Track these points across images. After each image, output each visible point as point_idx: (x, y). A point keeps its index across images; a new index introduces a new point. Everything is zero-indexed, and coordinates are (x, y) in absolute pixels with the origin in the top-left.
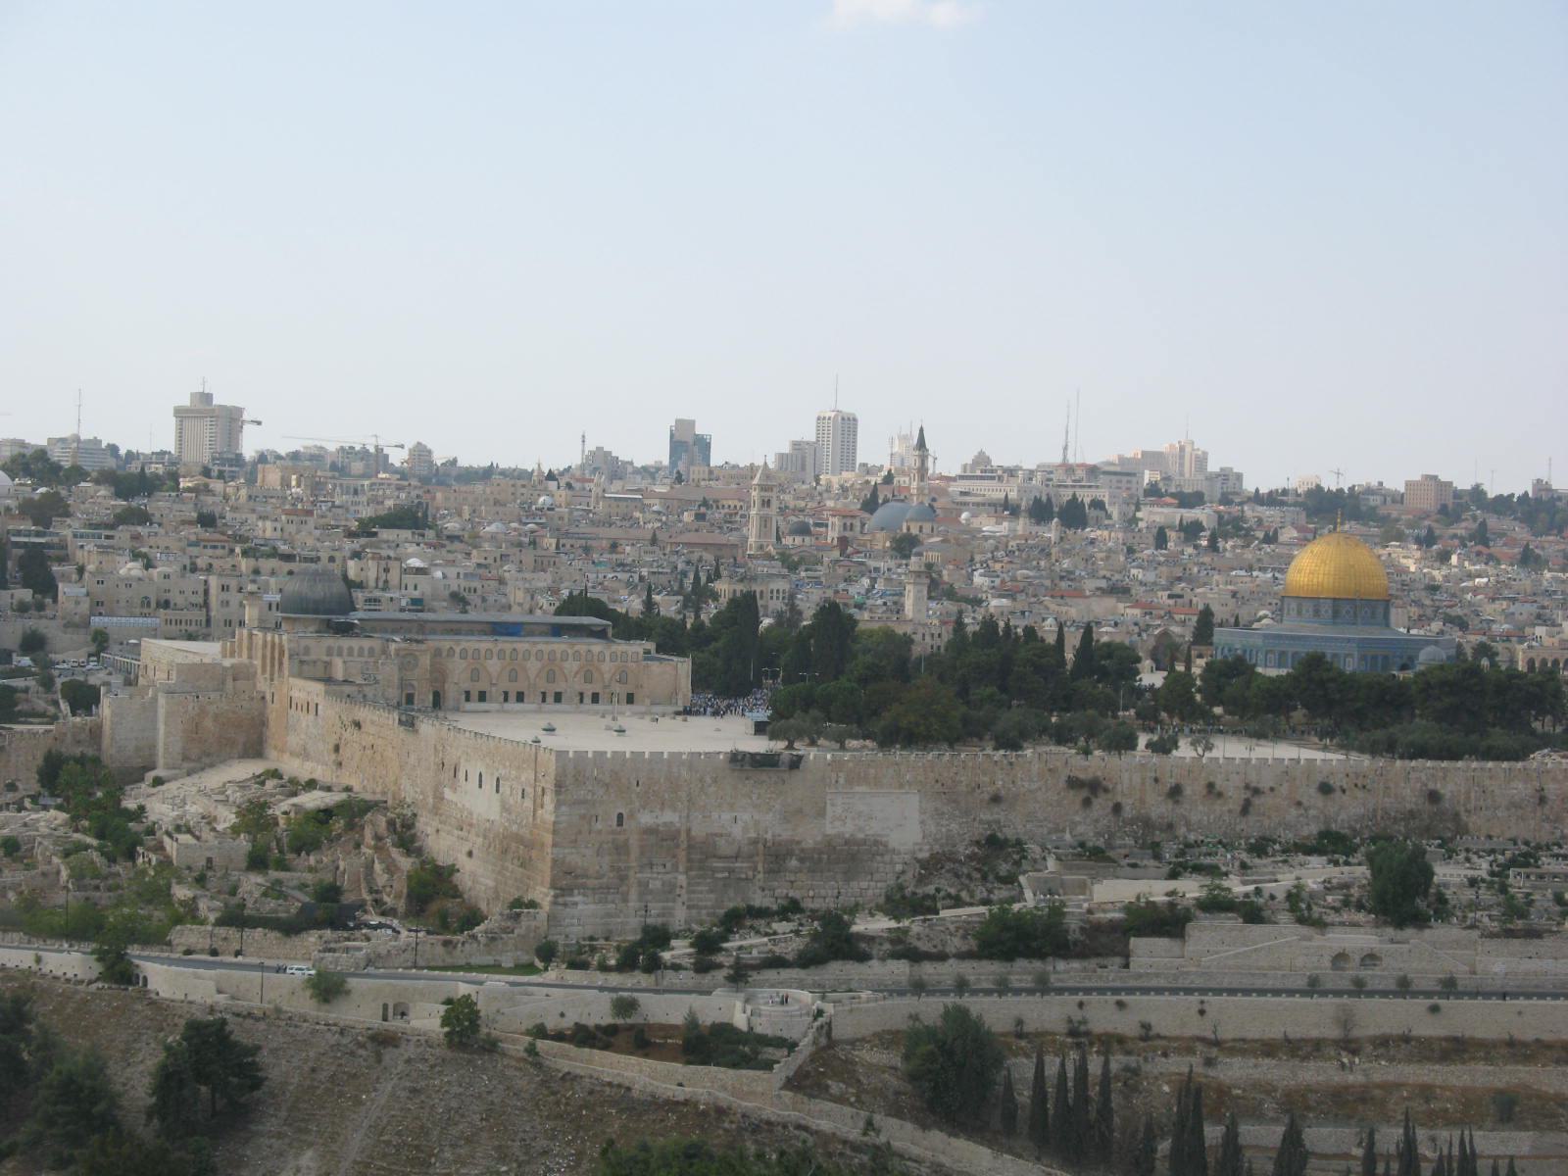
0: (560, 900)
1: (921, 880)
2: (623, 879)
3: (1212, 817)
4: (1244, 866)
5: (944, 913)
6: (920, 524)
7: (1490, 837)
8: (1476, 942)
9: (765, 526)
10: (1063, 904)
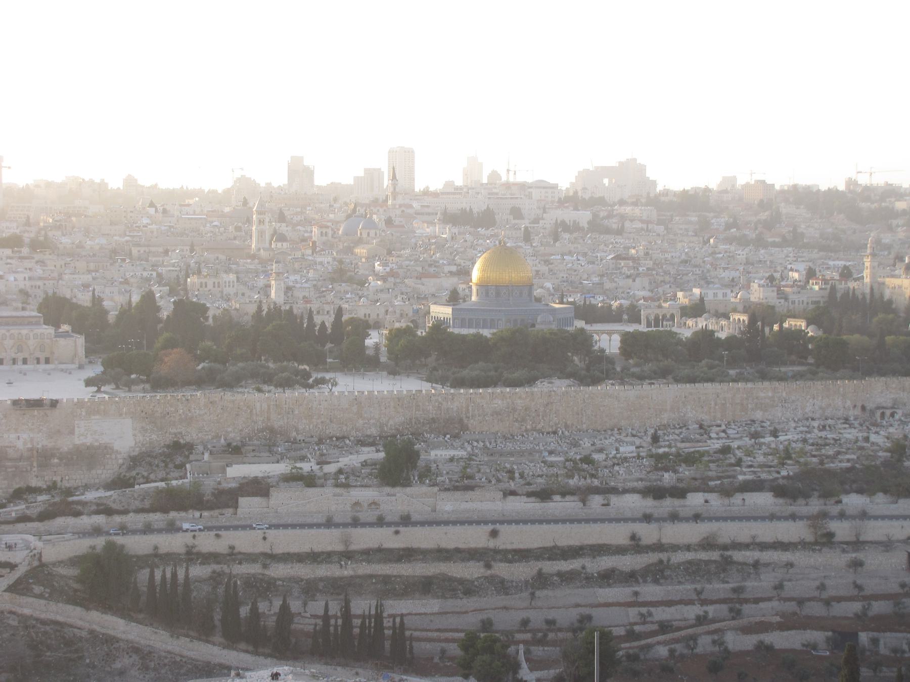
1: (130, 469)
3: (311, 426)
6: (368, 231)
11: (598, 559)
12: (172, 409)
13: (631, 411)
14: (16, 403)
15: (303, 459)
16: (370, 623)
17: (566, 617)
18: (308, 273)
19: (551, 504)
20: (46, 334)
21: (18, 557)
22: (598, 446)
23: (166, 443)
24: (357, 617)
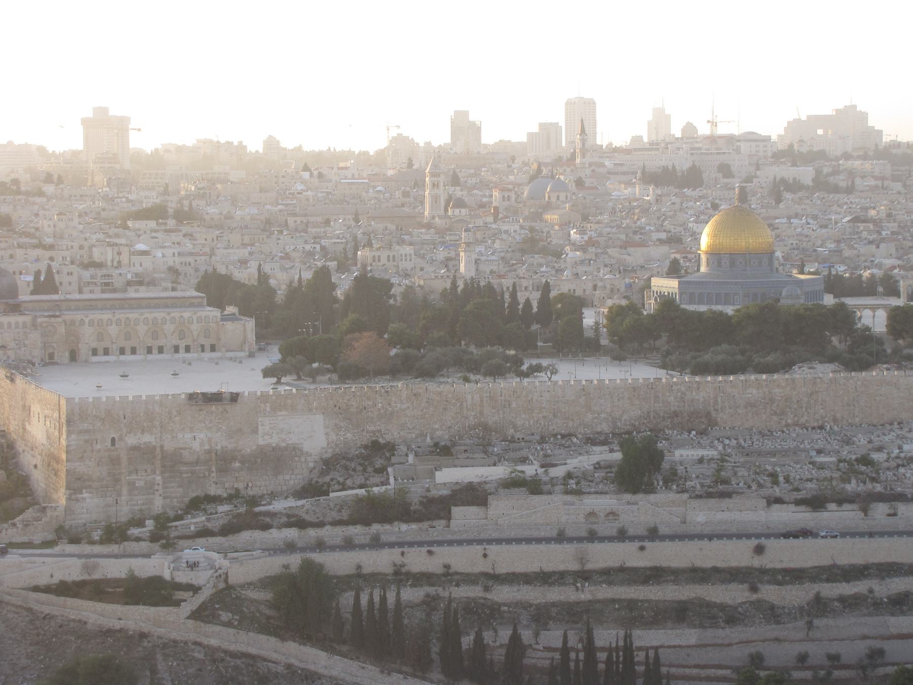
0: (73, 497)
1: (323, 473)
2: (117, 481)
3: (532, 422)
5: (332, 495)
8: (686, 501)
9: (436, 202)
11: (888, 580)
12: (369, 403)
14: (192, 397)
15: (524, 460)
16: (618, 657)
17: (854, 651)
18: (494, 243)
19: (826, 514)
20: (211, 317)
21: (201, 577)
22: (877, 444)
23: (364, 443)
24: (602, 649)
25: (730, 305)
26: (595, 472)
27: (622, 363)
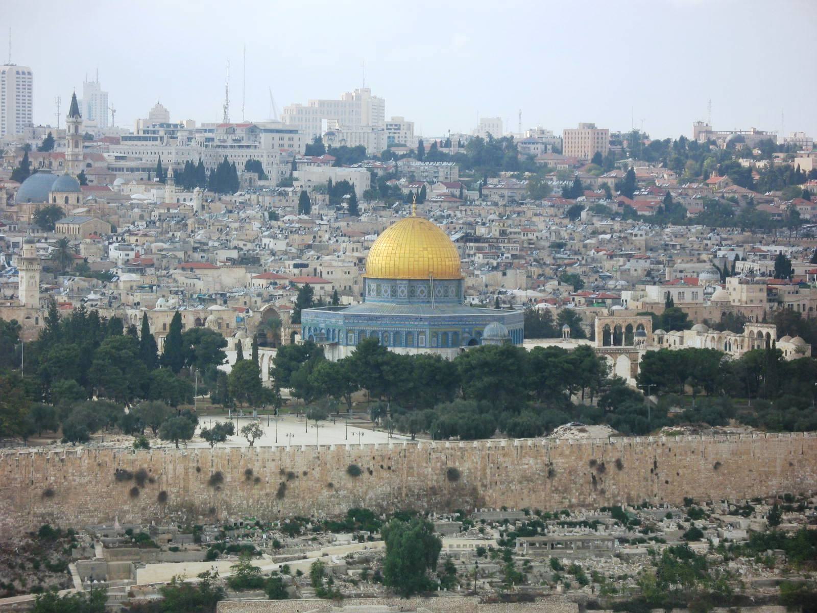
3: (251, 501)
4: (277, 545)
6: (65, 195)
7: (504, 509)
8: (476, 607)
10: (105, 588)
12: (38, 475)
13: (724, 475)
15: (251, 552)
23: (29, 531)
25: (413, 346)
26: (349, 569)
27: (320, 423)
